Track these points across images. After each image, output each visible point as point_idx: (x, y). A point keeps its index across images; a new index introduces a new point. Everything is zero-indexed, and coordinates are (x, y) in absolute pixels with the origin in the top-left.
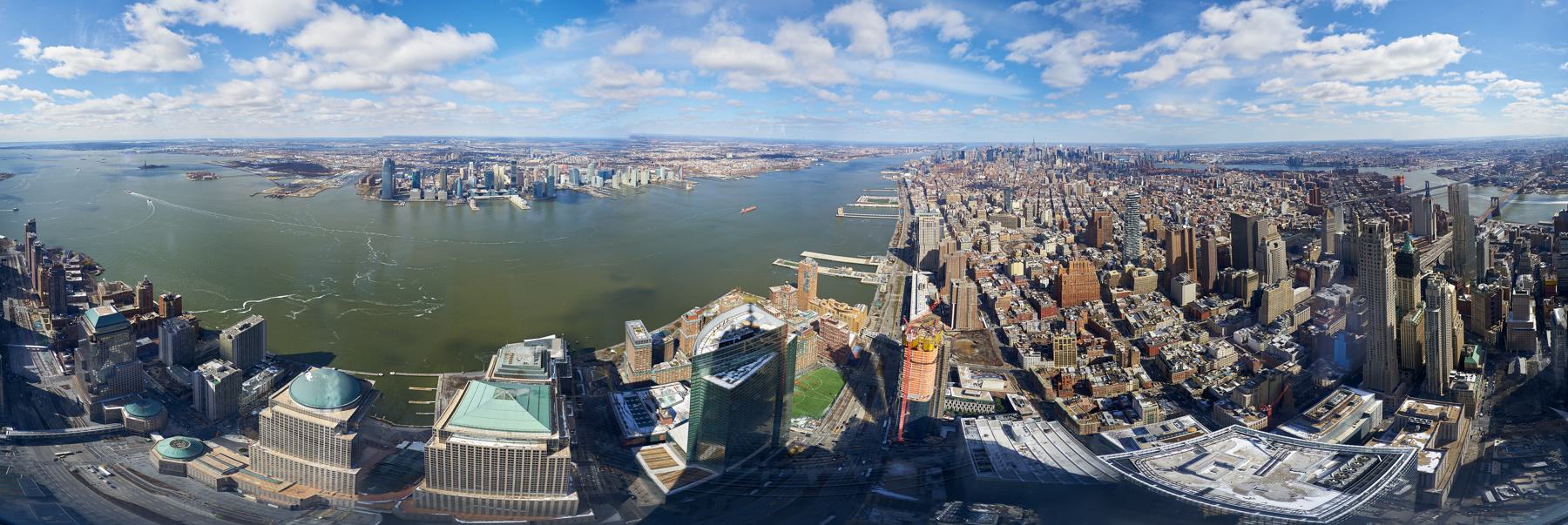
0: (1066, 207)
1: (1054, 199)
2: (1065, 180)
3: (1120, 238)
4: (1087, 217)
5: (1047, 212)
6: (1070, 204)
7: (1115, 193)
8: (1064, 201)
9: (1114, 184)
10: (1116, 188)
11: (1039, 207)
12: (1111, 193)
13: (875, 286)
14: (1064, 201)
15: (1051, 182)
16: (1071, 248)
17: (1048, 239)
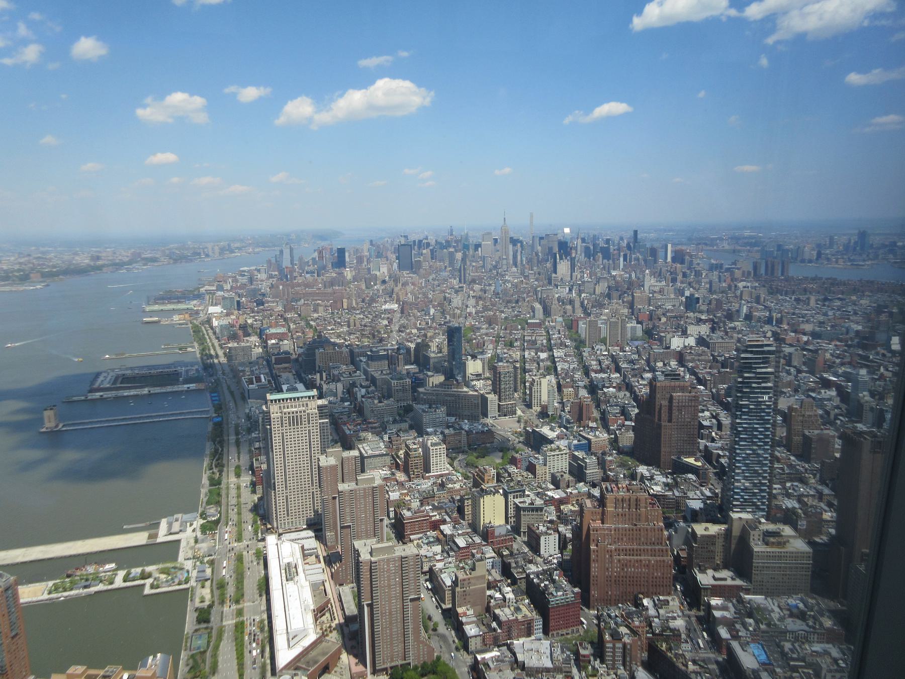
0: (586, 371)
1: (557, 353)
2: (579, 313)
3: (716, 448)
4: (636, 398)
5: (545, 382)
7: (701, 341)
8: (580, 356)
9: (699, 321)
10: (704, 329)
11: (524, 371)
12: (691, 341)
13: (183, 595)
14: (580, 356)
15: (547, 312)
16: (602, 464)
17: (551, 442)
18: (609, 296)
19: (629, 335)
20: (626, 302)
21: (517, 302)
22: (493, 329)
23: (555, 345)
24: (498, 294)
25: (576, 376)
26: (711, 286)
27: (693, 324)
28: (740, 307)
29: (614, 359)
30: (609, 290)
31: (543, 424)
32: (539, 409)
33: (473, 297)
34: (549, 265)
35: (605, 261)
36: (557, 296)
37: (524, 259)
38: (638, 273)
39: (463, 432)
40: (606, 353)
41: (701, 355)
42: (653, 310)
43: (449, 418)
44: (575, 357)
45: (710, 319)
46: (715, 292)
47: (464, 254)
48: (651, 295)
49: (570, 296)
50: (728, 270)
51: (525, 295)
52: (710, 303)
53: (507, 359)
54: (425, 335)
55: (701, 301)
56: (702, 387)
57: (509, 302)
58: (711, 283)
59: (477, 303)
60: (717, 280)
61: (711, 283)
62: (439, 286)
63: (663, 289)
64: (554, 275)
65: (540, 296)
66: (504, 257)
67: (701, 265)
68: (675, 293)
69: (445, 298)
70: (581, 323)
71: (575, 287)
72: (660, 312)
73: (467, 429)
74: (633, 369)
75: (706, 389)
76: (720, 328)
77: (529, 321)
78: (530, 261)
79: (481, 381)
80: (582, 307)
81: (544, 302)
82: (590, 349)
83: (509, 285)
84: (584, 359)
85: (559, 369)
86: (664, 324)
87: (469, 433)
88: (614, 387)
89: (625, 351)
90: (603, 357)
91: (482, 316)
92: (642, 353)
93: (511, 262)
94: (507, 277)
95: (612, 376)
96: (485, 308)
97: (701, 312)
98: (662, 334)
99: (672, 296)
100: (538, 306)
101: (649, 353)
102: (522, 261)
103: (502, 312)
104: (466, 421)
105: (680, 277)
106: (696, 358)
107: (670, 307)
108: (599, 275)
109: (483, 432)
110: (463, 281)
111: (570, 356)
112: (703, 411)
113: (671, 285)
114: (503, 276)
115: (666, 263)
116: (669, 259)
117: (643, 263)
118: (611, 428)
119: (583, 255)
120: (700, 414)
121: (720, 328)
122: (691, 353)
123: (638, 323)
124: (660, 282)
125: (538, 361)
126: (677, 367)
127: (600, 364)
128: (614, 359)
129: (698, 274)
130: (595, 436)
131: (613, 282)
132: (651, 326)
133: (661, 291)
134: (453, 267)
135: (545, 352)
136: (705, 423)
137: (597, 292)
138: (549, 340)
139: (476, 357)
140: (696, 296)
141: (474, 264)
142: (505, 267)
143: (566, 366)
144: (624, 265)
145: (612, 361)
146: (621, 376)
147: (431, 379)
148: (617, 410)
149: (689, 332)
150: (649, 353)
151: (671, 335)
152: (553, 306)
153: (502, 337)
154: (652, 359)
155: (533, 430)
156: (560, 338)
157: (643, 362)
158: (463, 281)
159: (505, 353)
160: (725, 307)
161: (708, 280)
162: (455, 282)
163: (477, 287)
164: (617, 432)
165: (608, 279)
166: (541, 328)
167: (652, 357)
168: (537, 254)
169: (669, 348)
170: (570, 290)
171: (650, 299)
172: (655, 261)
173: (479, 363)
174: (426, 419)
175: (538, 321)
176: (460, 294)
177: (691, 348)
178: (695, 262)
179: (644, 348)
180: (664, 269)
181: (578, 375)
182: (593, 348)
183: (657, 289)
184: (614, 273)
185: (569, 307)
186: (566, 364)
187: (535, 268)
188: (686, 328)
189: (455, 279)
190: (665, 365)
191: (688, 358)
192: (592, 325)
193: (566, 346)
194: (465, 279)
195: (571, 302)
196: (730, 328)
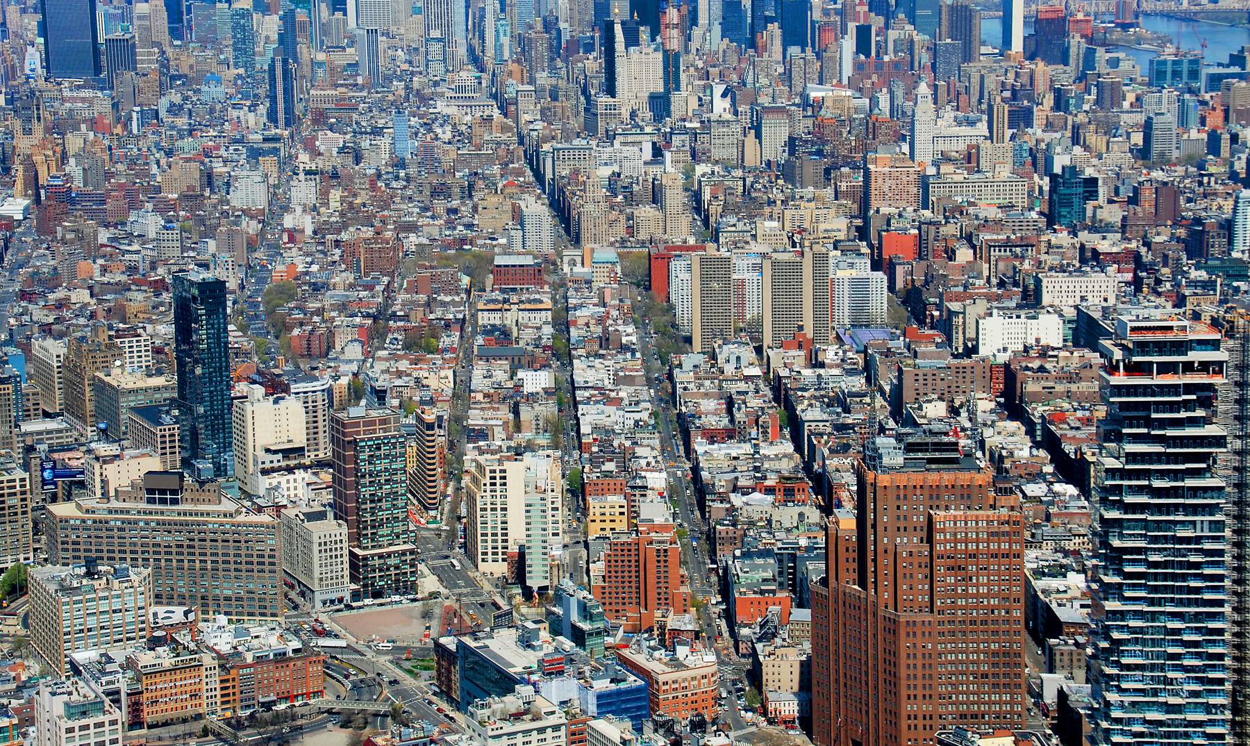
1: (586, 372)
2: (682, 230)
6: (710, 412)
9: (1092, 259)
18: (788, 172)
19: (844, 314)
20: (846, 195)
21: (469, 191)
22: (369, 287)
23: (583, 341)
24: (401, 164)
25: (639, 451)
26: (1147, 139)
27: (1062, 269)
28: (1235, 210)
29: (782, 394)
30: (792, 153)
31: (504, 619)
32: (501, 569)
33: (308, 173)
34: (592, 63)
35: (794, 50)
36: (605, 172)
37: (505, 40)
38: (899, 93)
39: (208, 659)
40: (756, 371)
41: (1072, 378)
42: (930, 223)
43: (161, 610)
44: (649, 382)
45: (1128, 252)
46: (1164, 162)
47: (288, 19)
48: (931, 171)
49: (655, 170)
50: (1215, 81)
51: (496, 169)
52: (1134, 200)
53: (406, 393)
54: (119, 312)
55: (1102, 191)
56: (1071, 490)
57: (440, 191)
58: (1148, 127)
59: (324, 195)
60: (1171, 118)
61: (1148, 127)
62: (191, 133)
63: (978, 147)
64: (604, 99)
65: (549, 175)
66: (436, 34)
67: (1125, 66)
68: (1018, 161)
69: (209, 179)
70: (678, 269)
71: (676, 140)
72: (950, 230)
73: (225, 649)
74: (841, 428)
75: (1085, 491)
76: (1158, 282)
77: (499, 261)
78: (523, 43)
79: (300, 474)
80: (698, 210)
81: (562, 191)
82: (699, 359)
83: (446, 133)
84: (679, 391)
85: (585, 429)
86: (967, 268)
87: (226, 662)
88: (769, 491)
89: (822, 365)
90: (742, 386)
91: (337, 243)
92: (881, 369)
93: (462, 51)
94: (441, 107)
95: (766, 450)
96: (351, 214)
97: (1099, 228)
98: (955, 306)
99: (1005, 172)
100: (535, 207)
101: (900, 371)
102: (499, 48)
103: (413, 228)
104: (222, 619)
105: (1044, 109)
106: (1060, 388)
107: (993, 213)
108: (765, 100)
109: (281, 657)
110: (281, 115)
111: (629, 380)
112: (1060, 571)
113: (1009, 133)
114: (424, 99)
115: (1008, 58)
116: (1017, 45)
117: (926, 58)
118: (745, 631)
119: (717, 29)
120: (1055, 583)
121: (1158, 282)
122: (1042, 369)
123: (876, 266)
124: (972, 123)
125: (515, 400)
126: (994, 417)
127: (730, 411)
128: (782, 394)
129: (1109, 96)
130: (677, 664)
131: (810, 122)
132: (919, 279)
133: (971, 159)
134: (249, 65)
135: (545, 366)
136: (1064, 614)
137: (751, 159)
138: (562, 324)
139: (286, 389)
140: (1089, 172)
141: (321, 57)
142: (437, 69)
143: (612, 417)
144: (858, 67)
145: (777, 399)
146: (799, 448)
147: (110, 470)
148: (766, 570)
149: (1046, 299)
150: (900, 371)
151: (982, 305)
152: (590, 207)
153: (394, 316)
154: (908, 395)
155: (462, 646)
156: (601, 321)
157: (879, 401)
158: (281, 115)
159: (399, 374)
160: (1189, 211)
161: (1140, 118)
162: (253, 121)
163: (329, 141)
164: (759, 646)
165: (790, 116)
166: (541, 283)
167: (908, 382)
168: (550, 25)
169: (971, 351)
170: (657, 152)
171: (924, 182)
172: (968, 56)
173: (293, 407)
174: (70, 615)
175: (529, 260)
176: (269, 164)
177: (1044, 353)
178: (1101, 55)
179: (888, 353)
180: (991, 83)
181: (647, 452)
182: (714, 357)
183: (957, 148)
184: (815, 93)
185: (646, 212)
186: (611, 409)
187: (543, 78)
188: (1038, 282)
189: (253, 108)
190: (954, 411)
191: (1031, 387)
192: (715, 271)
193: (624, 348)
194: (289, 110)
195: (656, 195)
196: (1194, 284)
